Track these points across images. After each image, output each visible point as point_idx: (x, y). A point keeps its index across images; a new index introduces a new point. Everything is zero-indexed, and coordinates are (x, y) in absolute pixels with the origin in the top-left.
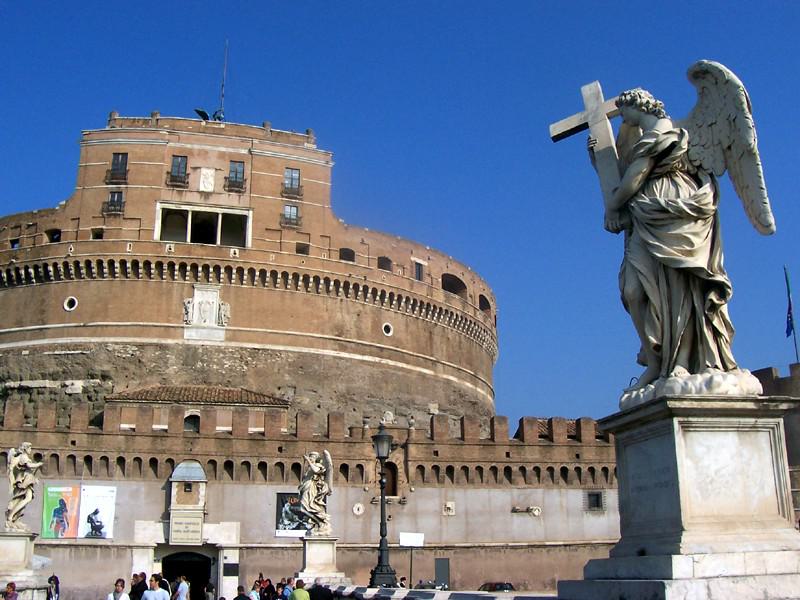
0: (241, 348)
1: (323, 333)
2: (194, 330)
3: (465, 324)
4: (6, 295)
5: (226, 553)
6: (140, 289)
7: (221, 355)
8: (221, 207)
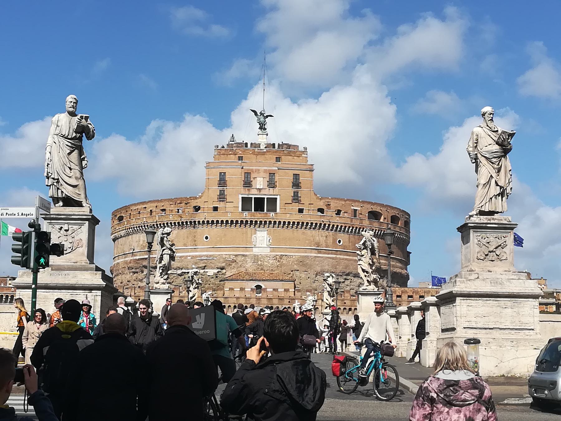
0: (277, 255)
1: (310, 246)
2: (257, 248)
4: (178, 232)
6: (234, 230)
7: (269, 258)
8: (266, 195)
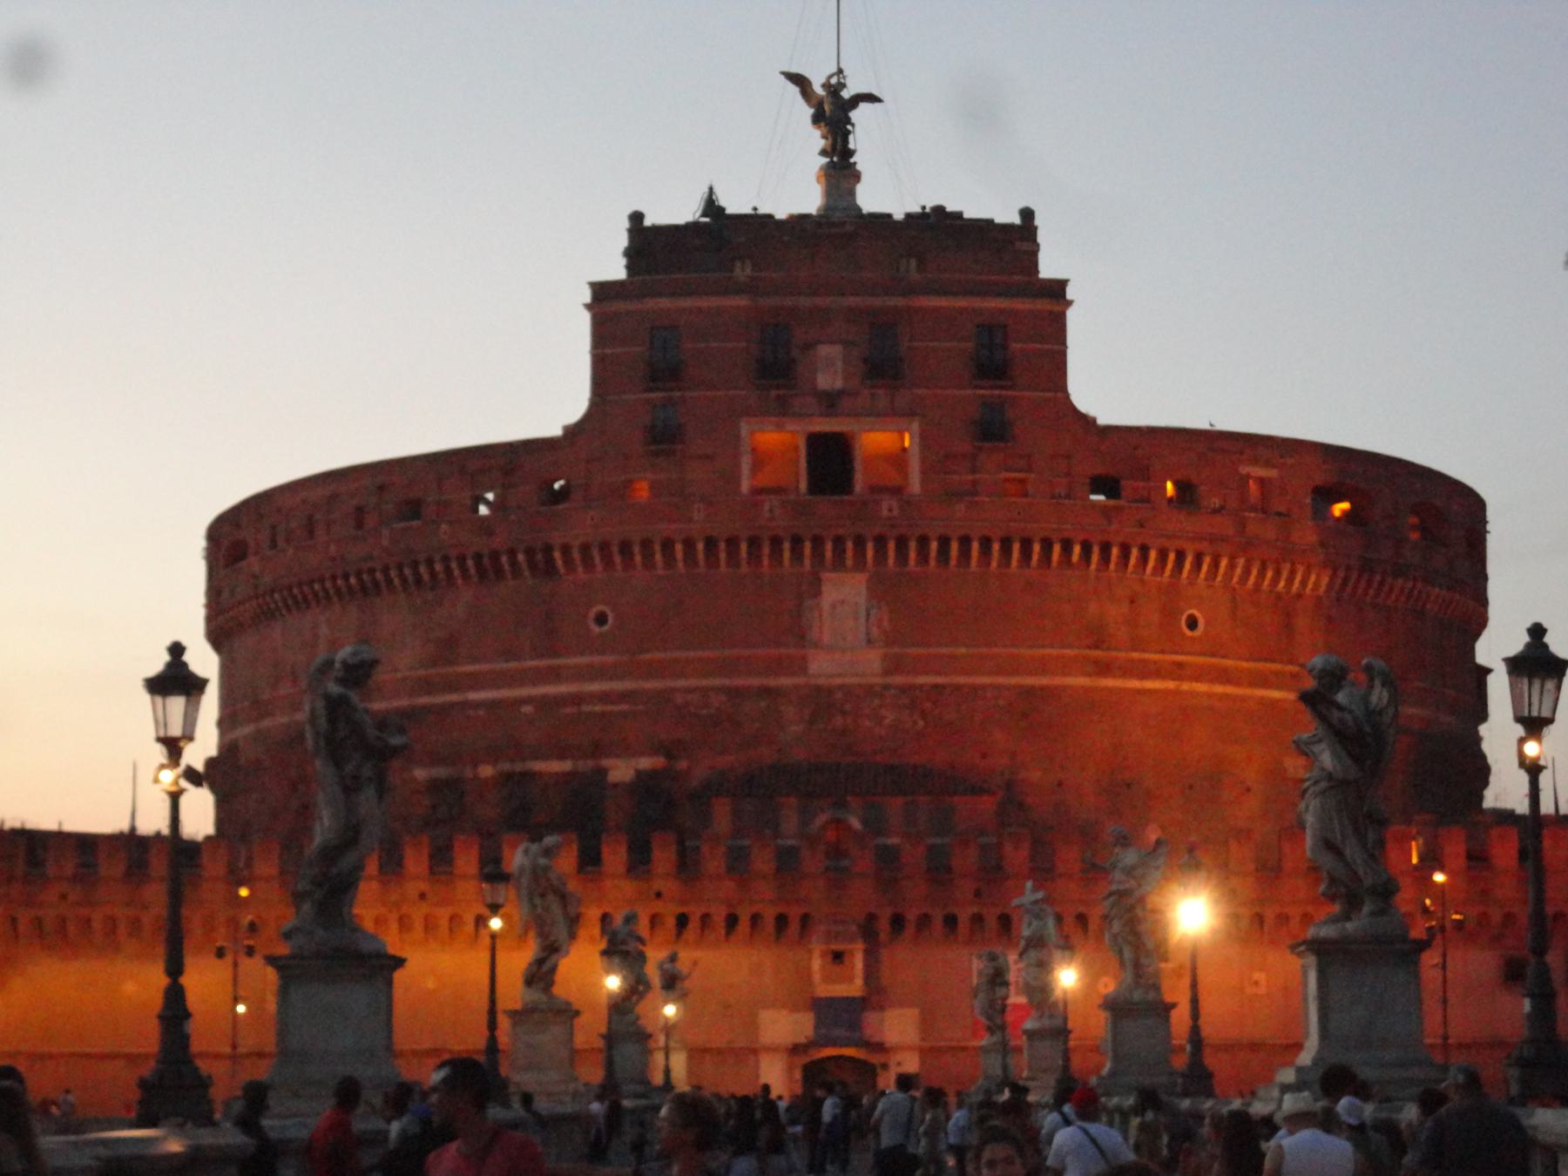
0: (912, 687)
3: (1369, 582)
5: (898, 1057)
7: (876, 702)
